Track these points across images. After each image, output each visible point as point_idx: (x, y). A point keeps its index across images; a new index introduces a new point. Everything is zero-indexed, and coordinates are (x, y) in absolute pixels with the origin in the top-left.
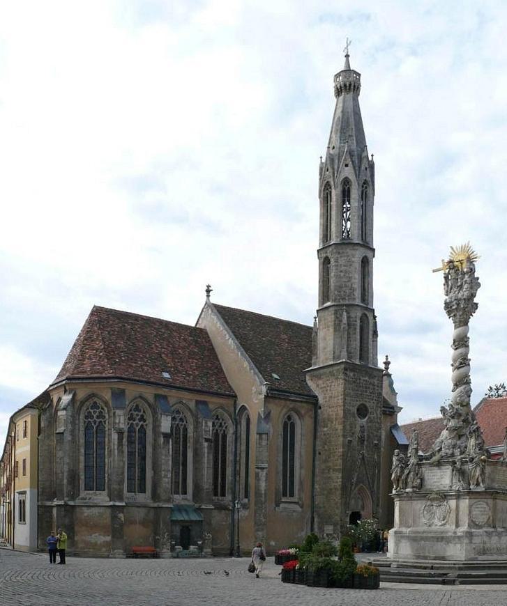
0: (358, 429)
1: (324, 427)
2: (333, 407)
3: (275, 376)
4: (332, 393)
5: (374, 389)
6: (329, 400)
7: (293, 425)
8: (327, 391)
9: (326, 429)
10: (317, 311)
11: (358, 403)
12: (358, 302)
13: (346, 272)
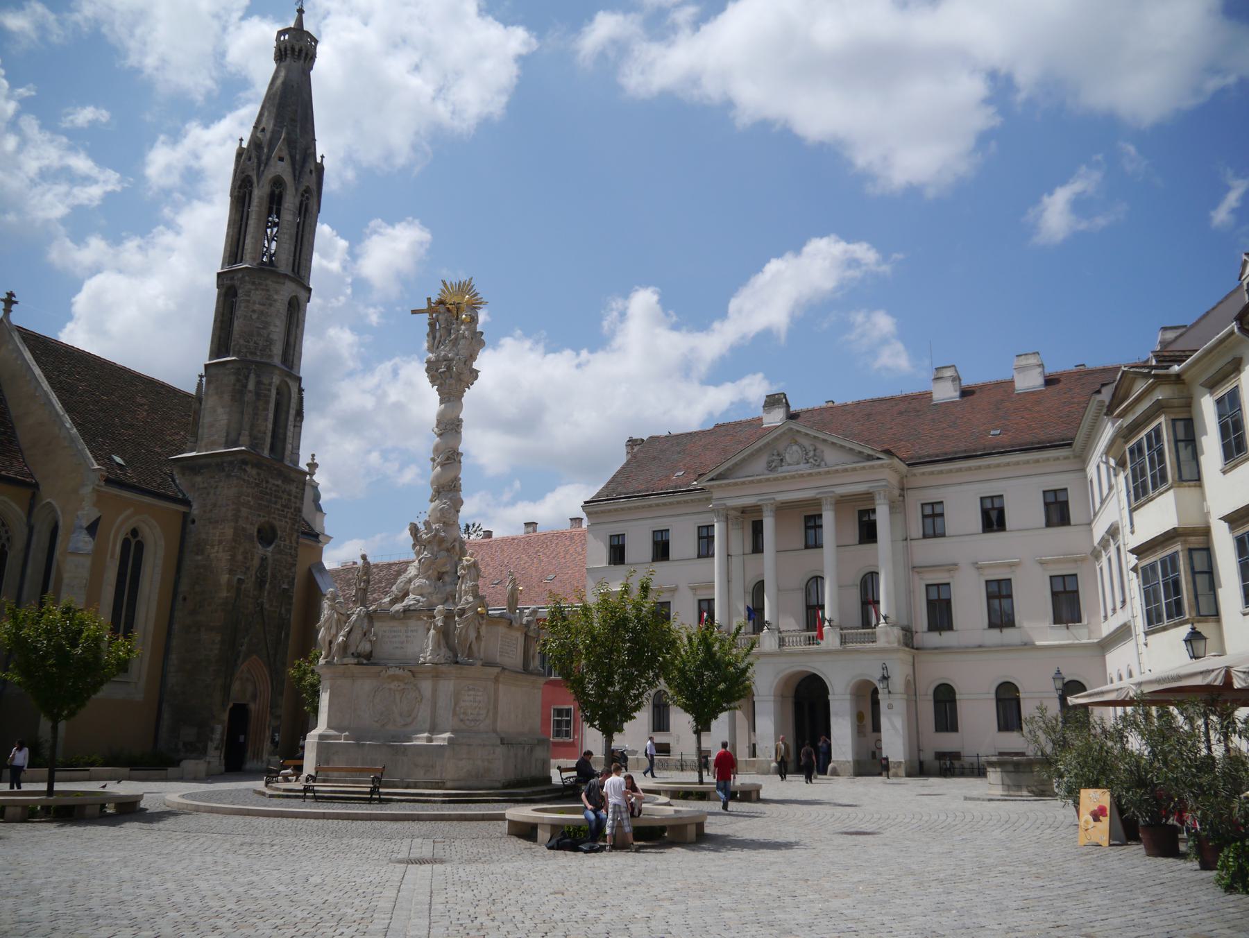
0: (256, 562)
3: (118, 460)
7: (140, 547)
8: (208, 494)
9: (200, 558)
10: (207, 366)
11: (262, 520)
12: (277, 361)
13: (262, 313)
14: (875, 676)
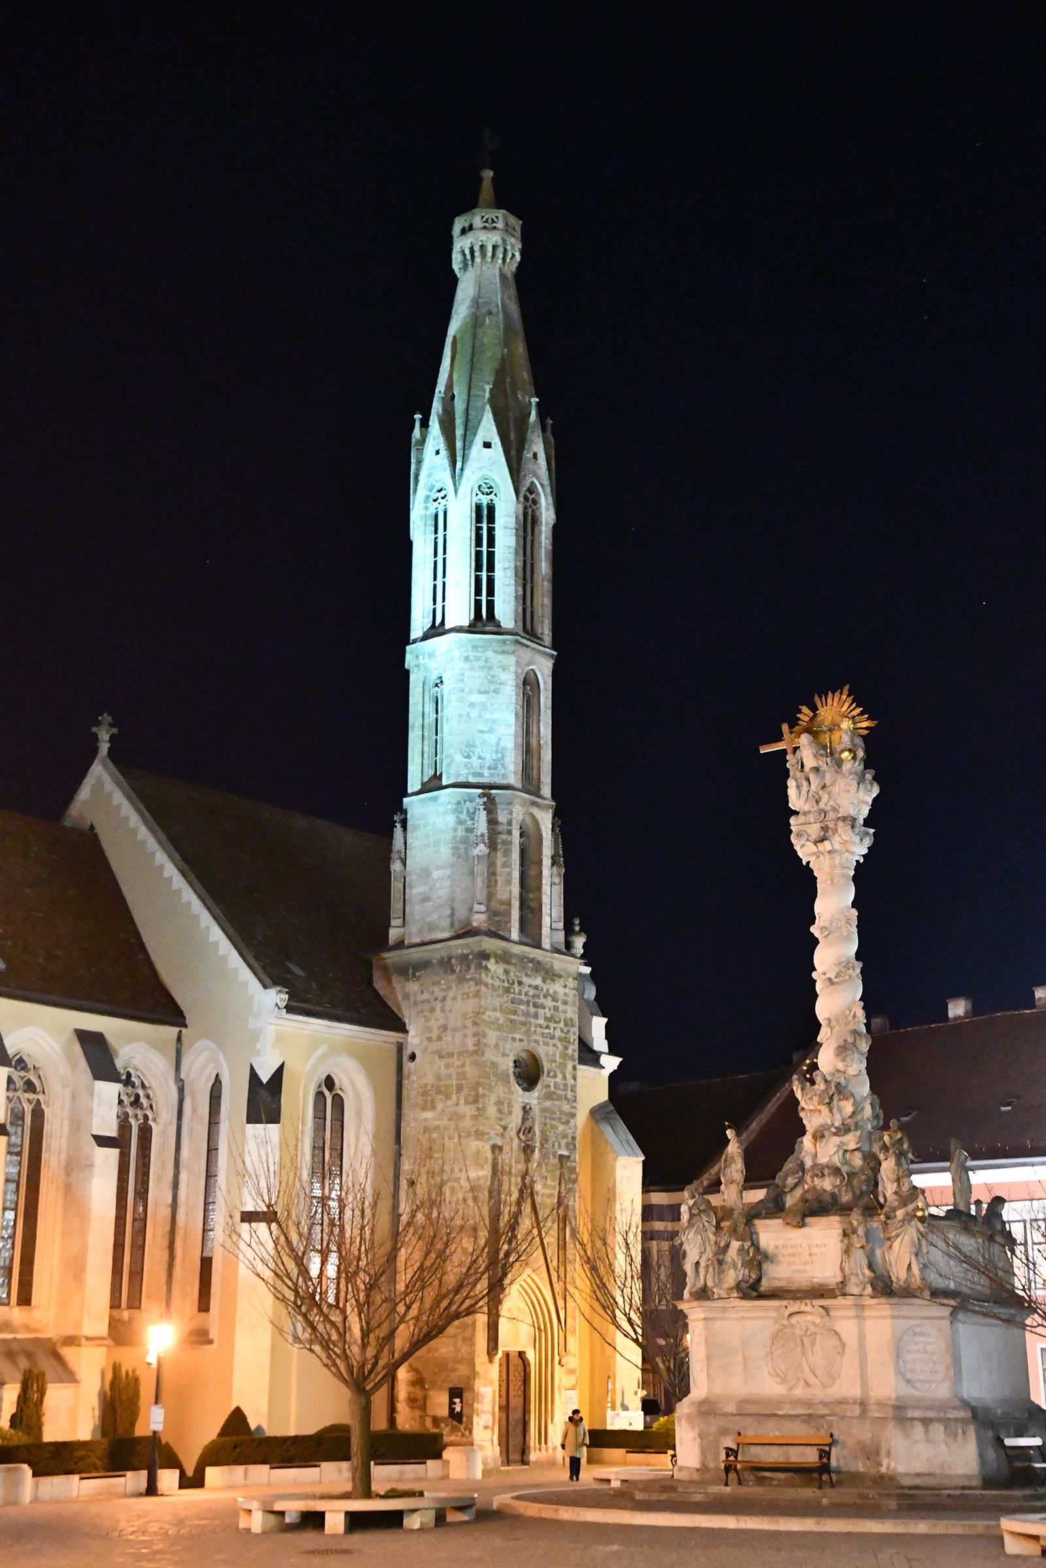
0: (517, 1114)
1: (424, 1109)
2: (451, 1055)
4: (446, 1018)
5: (556, 1008)
6: (439, 1038)
7: (339, 1103)
8: (433, 1010)
9: (429, 1115)
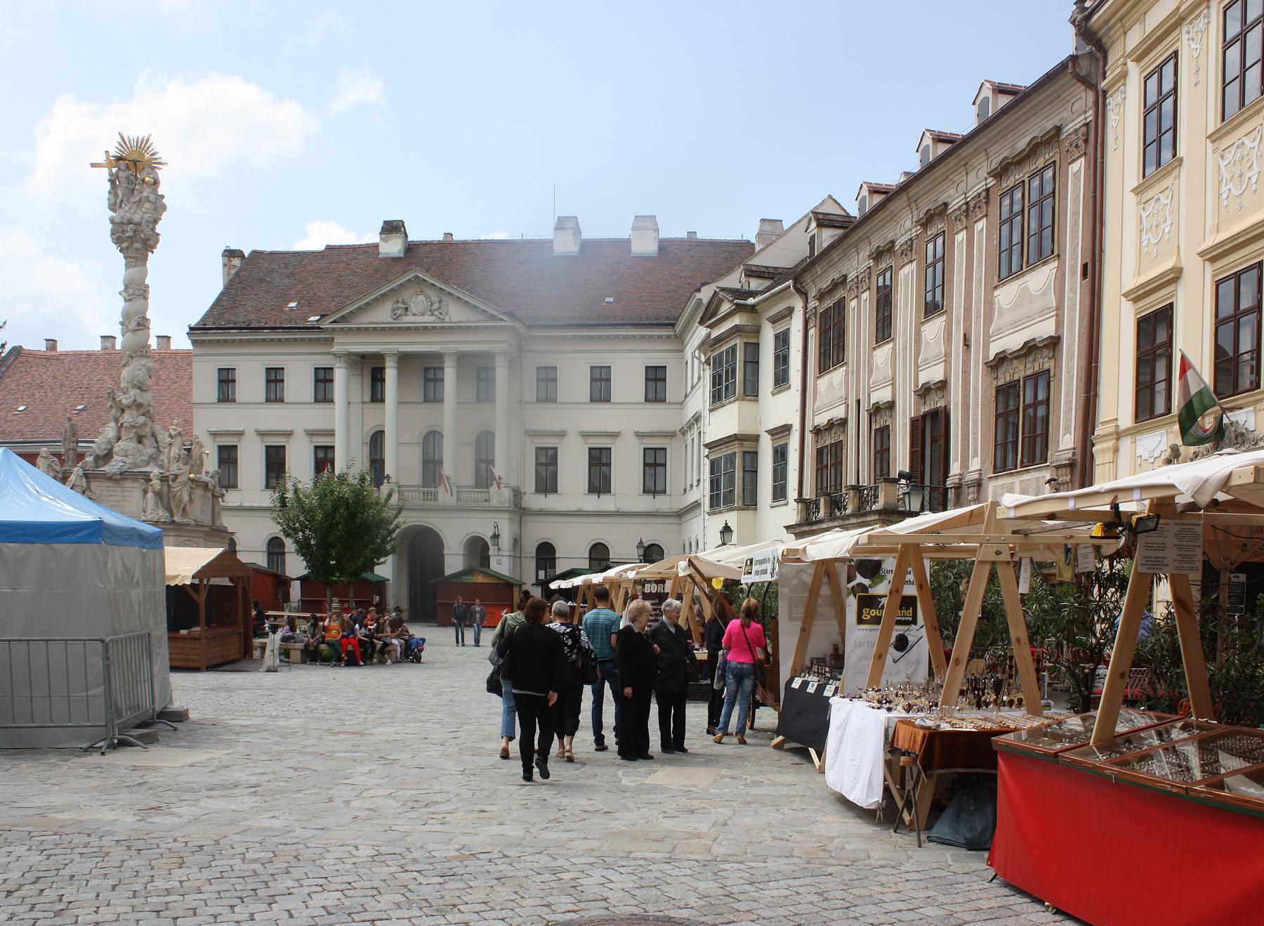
14: (487, 534)
